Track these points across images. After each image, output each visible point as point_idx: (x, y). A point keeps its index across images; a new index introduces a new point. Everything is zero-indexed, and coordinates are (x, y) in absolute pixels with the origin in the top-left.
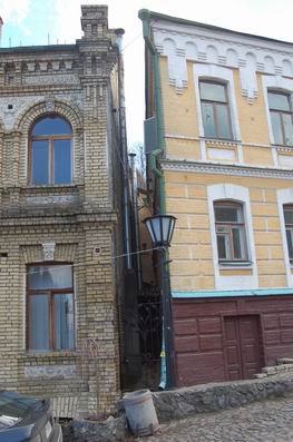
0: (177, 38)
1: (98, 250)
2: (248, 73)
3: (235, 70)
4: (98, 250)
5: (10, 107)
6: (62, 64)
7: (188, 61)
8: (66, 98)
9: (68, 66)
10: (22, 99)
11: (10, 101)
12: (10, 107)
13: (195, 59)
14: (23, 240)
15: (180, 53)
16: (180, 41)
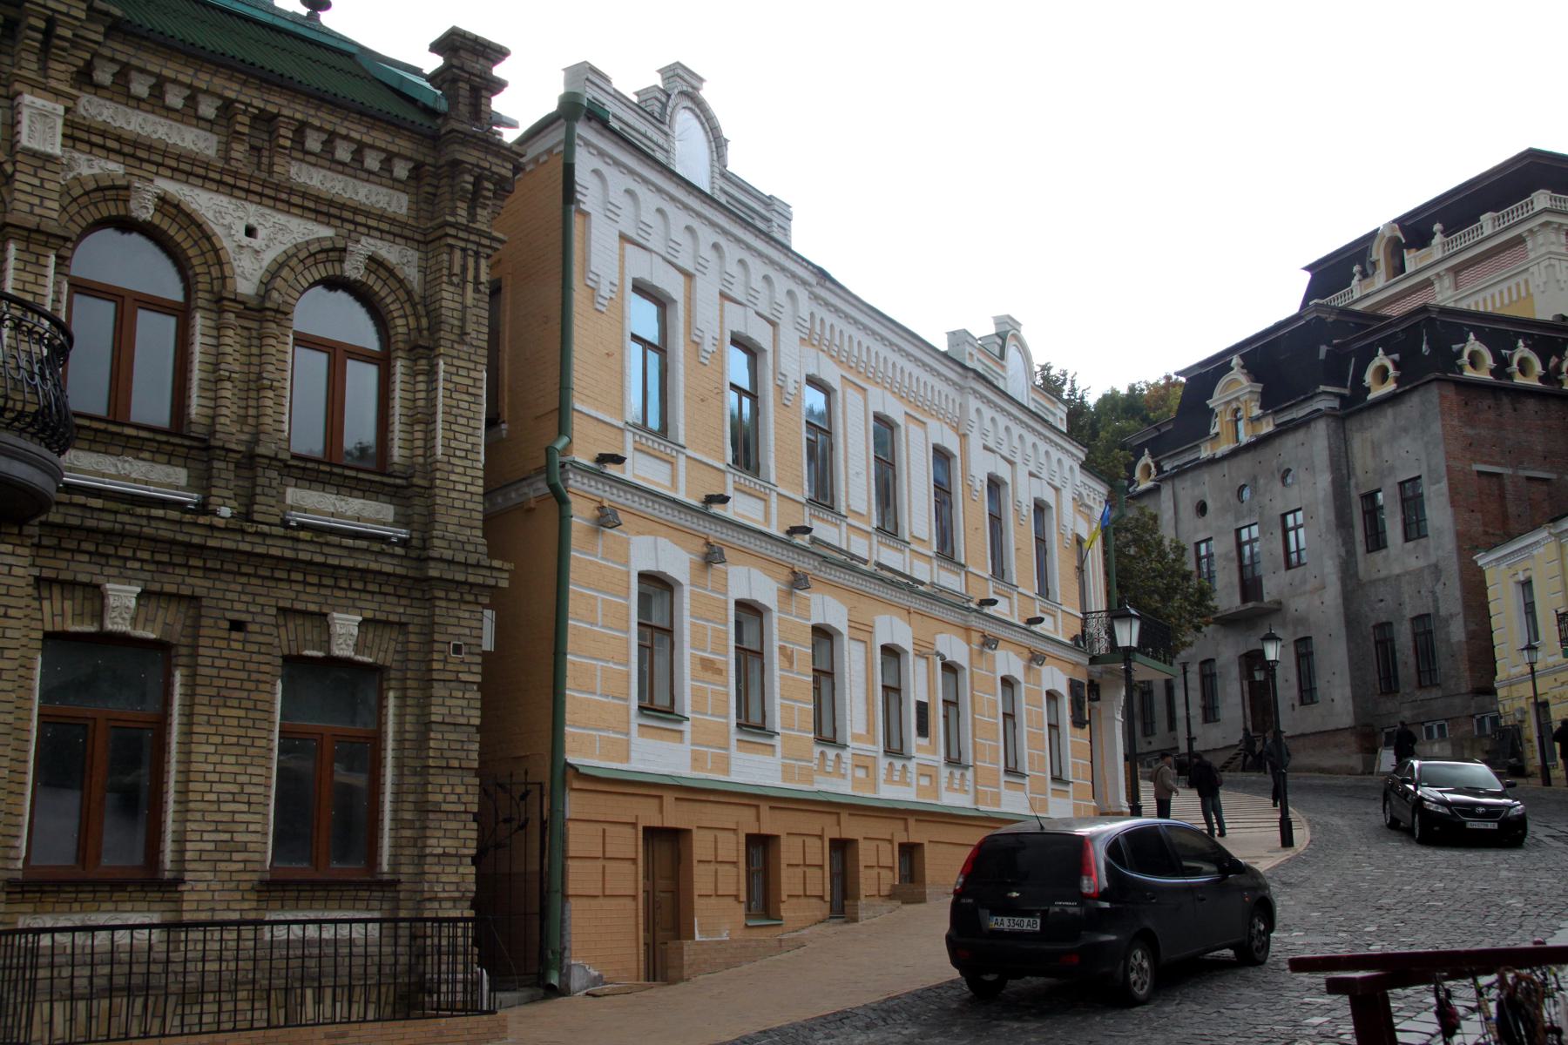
0: (611, 173)
1: (457, 649)
2: (707, 288)
3: (688, 276)
4: (457, 649)
5: (250, 232)
6: (389, 159)
7: (624, 238)
8: (390, 253)
9: (401, 170)
10: (282, 218)
11: (252, 213)
12: (250, 232)
13: (631, 233)
14: (286, 595)
15: (611, 211)
16: (618, 182)
